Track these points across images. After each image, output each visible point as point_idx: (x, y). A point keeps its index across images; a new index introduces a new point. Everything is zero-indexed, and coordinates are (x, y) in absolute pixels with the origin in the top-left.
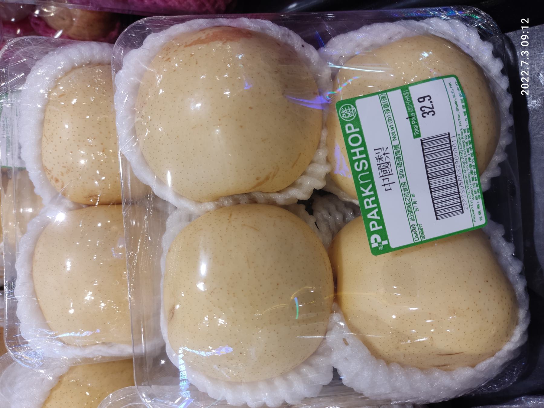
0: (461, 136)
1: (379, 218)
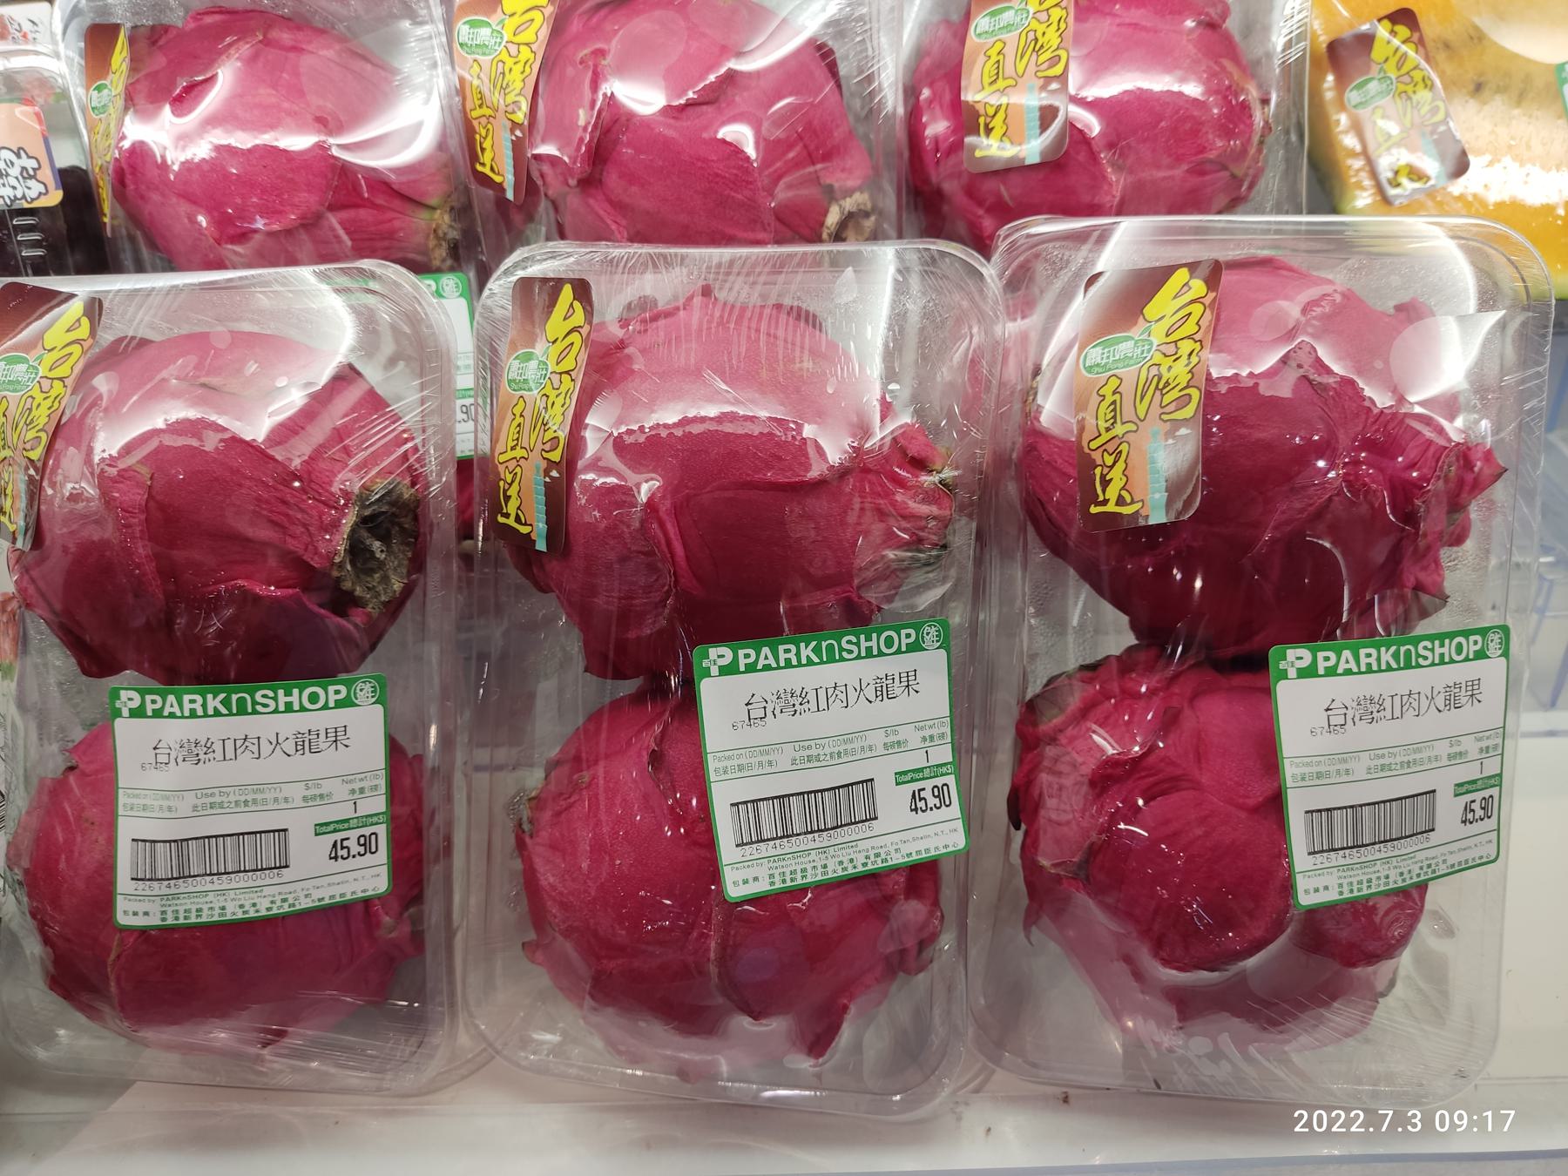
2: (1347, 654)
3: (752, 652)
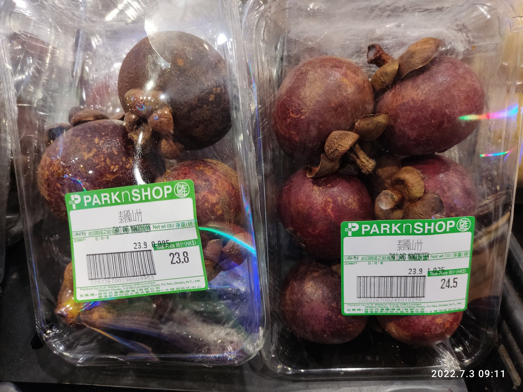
1: (93, 204)
2: (375, 226)
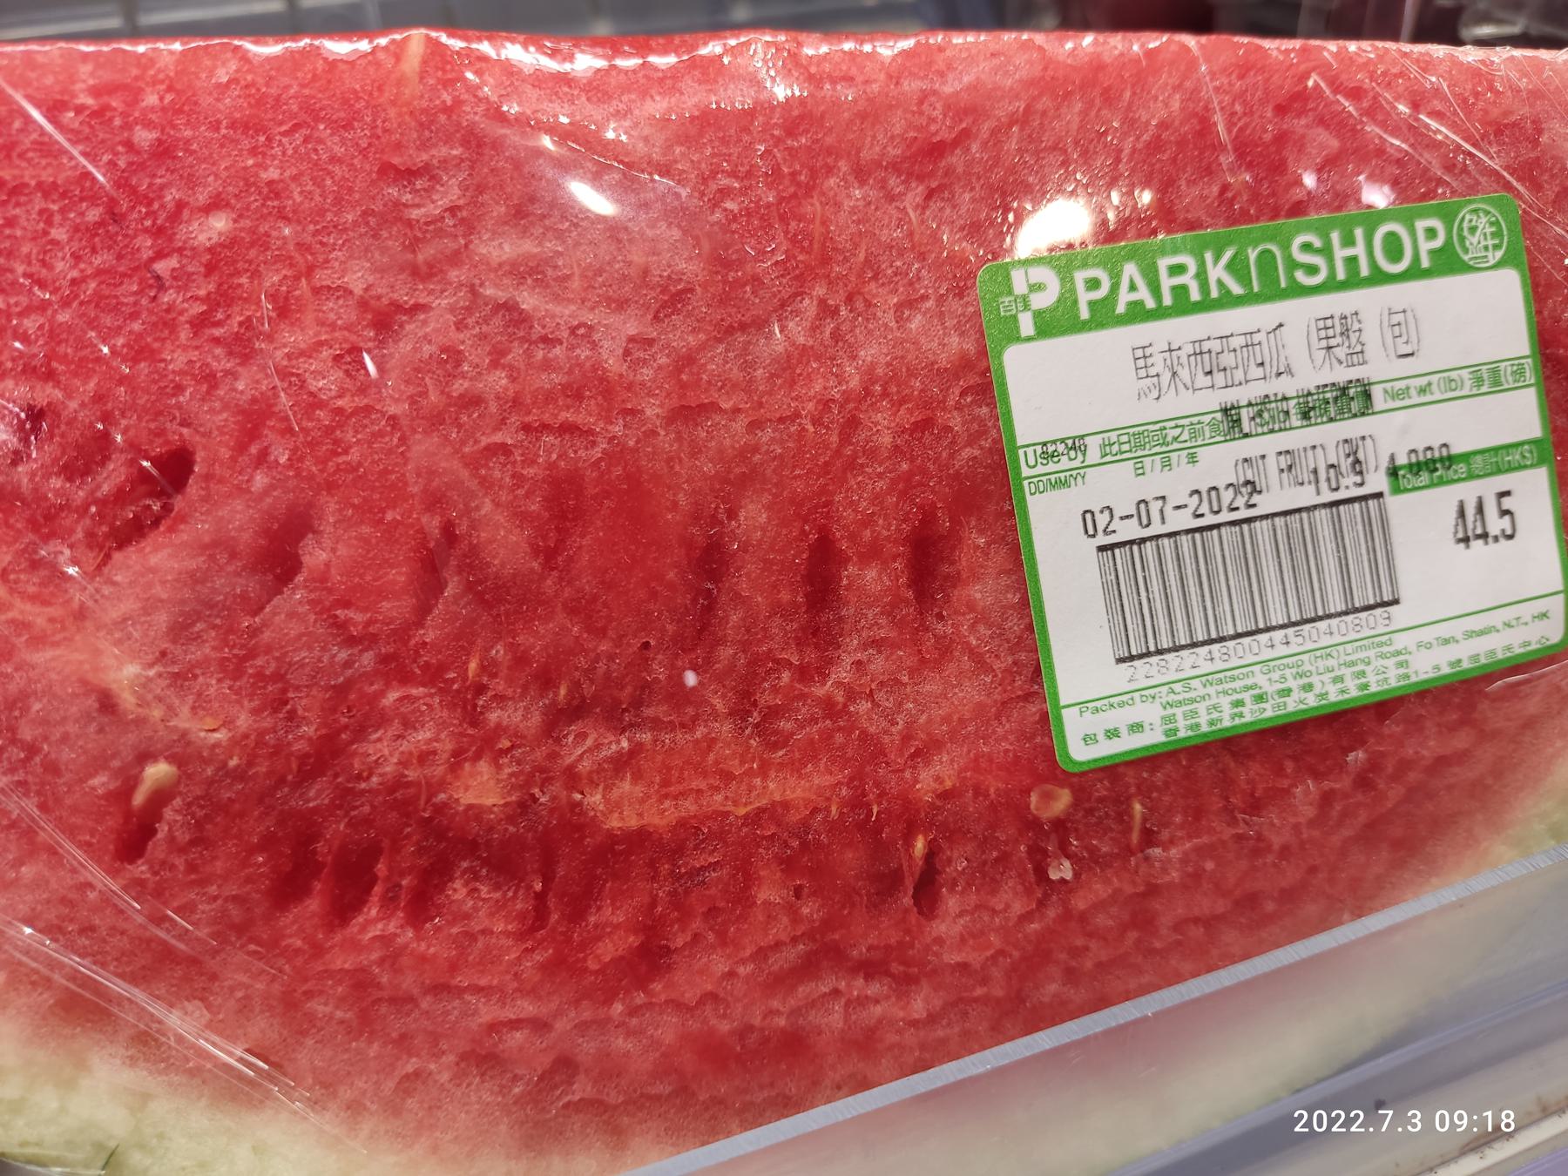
0: (1385, 649)
1: (1121, 309)
3: (1101, 274)
